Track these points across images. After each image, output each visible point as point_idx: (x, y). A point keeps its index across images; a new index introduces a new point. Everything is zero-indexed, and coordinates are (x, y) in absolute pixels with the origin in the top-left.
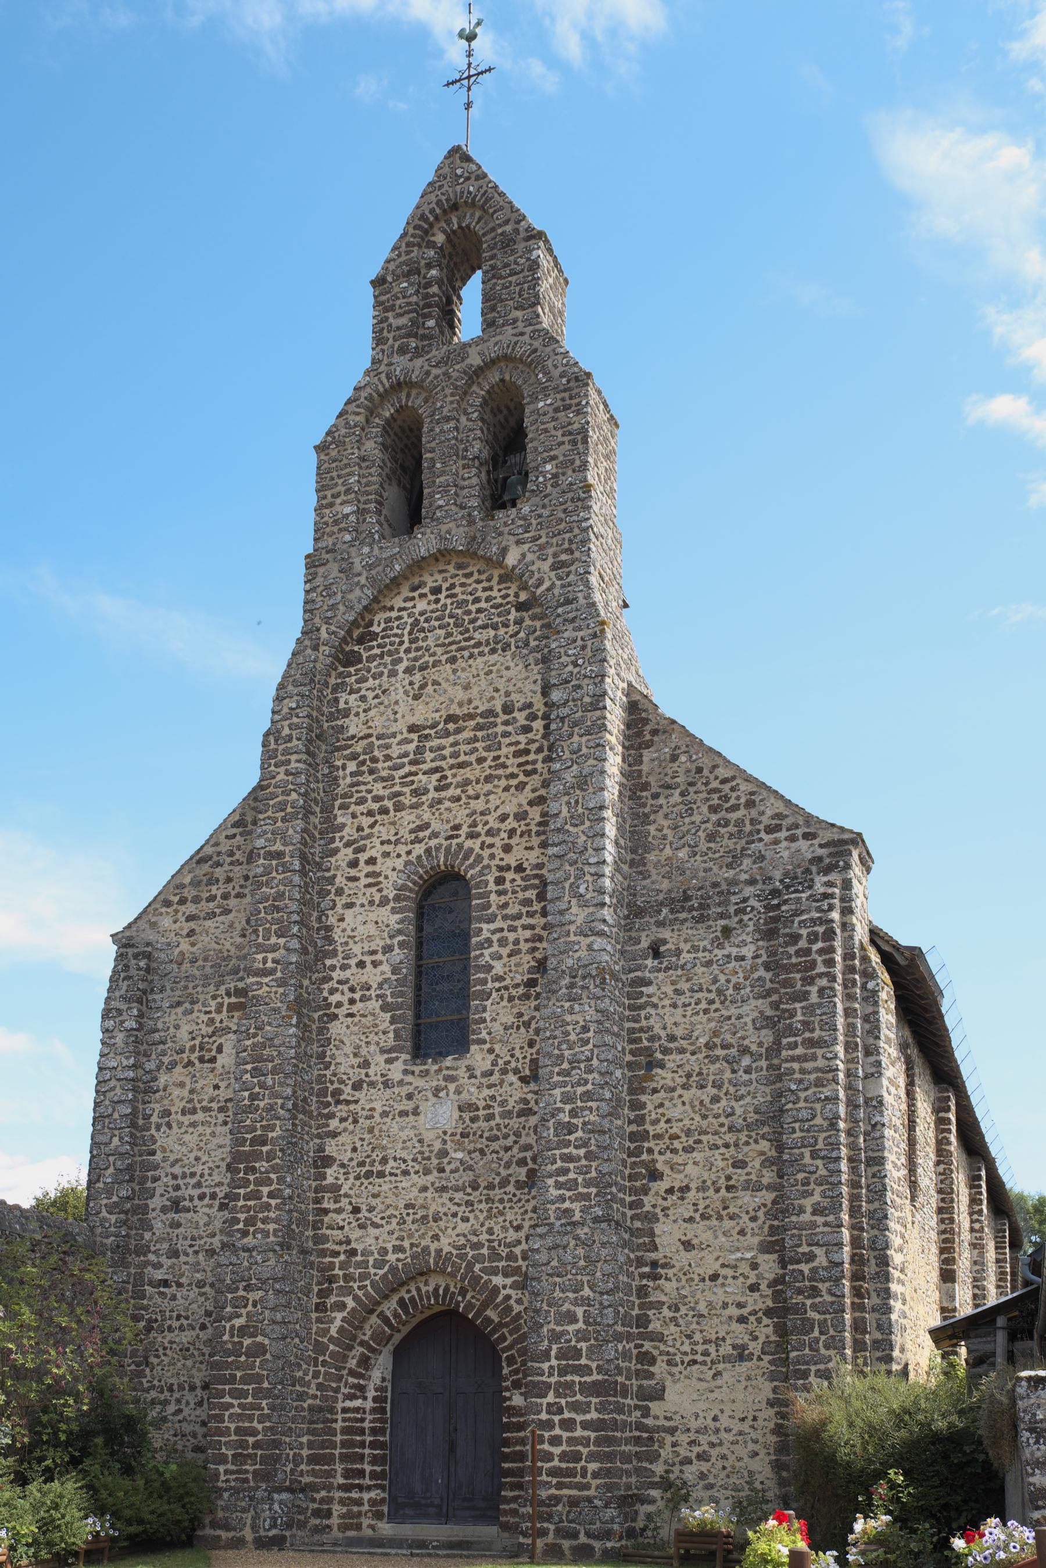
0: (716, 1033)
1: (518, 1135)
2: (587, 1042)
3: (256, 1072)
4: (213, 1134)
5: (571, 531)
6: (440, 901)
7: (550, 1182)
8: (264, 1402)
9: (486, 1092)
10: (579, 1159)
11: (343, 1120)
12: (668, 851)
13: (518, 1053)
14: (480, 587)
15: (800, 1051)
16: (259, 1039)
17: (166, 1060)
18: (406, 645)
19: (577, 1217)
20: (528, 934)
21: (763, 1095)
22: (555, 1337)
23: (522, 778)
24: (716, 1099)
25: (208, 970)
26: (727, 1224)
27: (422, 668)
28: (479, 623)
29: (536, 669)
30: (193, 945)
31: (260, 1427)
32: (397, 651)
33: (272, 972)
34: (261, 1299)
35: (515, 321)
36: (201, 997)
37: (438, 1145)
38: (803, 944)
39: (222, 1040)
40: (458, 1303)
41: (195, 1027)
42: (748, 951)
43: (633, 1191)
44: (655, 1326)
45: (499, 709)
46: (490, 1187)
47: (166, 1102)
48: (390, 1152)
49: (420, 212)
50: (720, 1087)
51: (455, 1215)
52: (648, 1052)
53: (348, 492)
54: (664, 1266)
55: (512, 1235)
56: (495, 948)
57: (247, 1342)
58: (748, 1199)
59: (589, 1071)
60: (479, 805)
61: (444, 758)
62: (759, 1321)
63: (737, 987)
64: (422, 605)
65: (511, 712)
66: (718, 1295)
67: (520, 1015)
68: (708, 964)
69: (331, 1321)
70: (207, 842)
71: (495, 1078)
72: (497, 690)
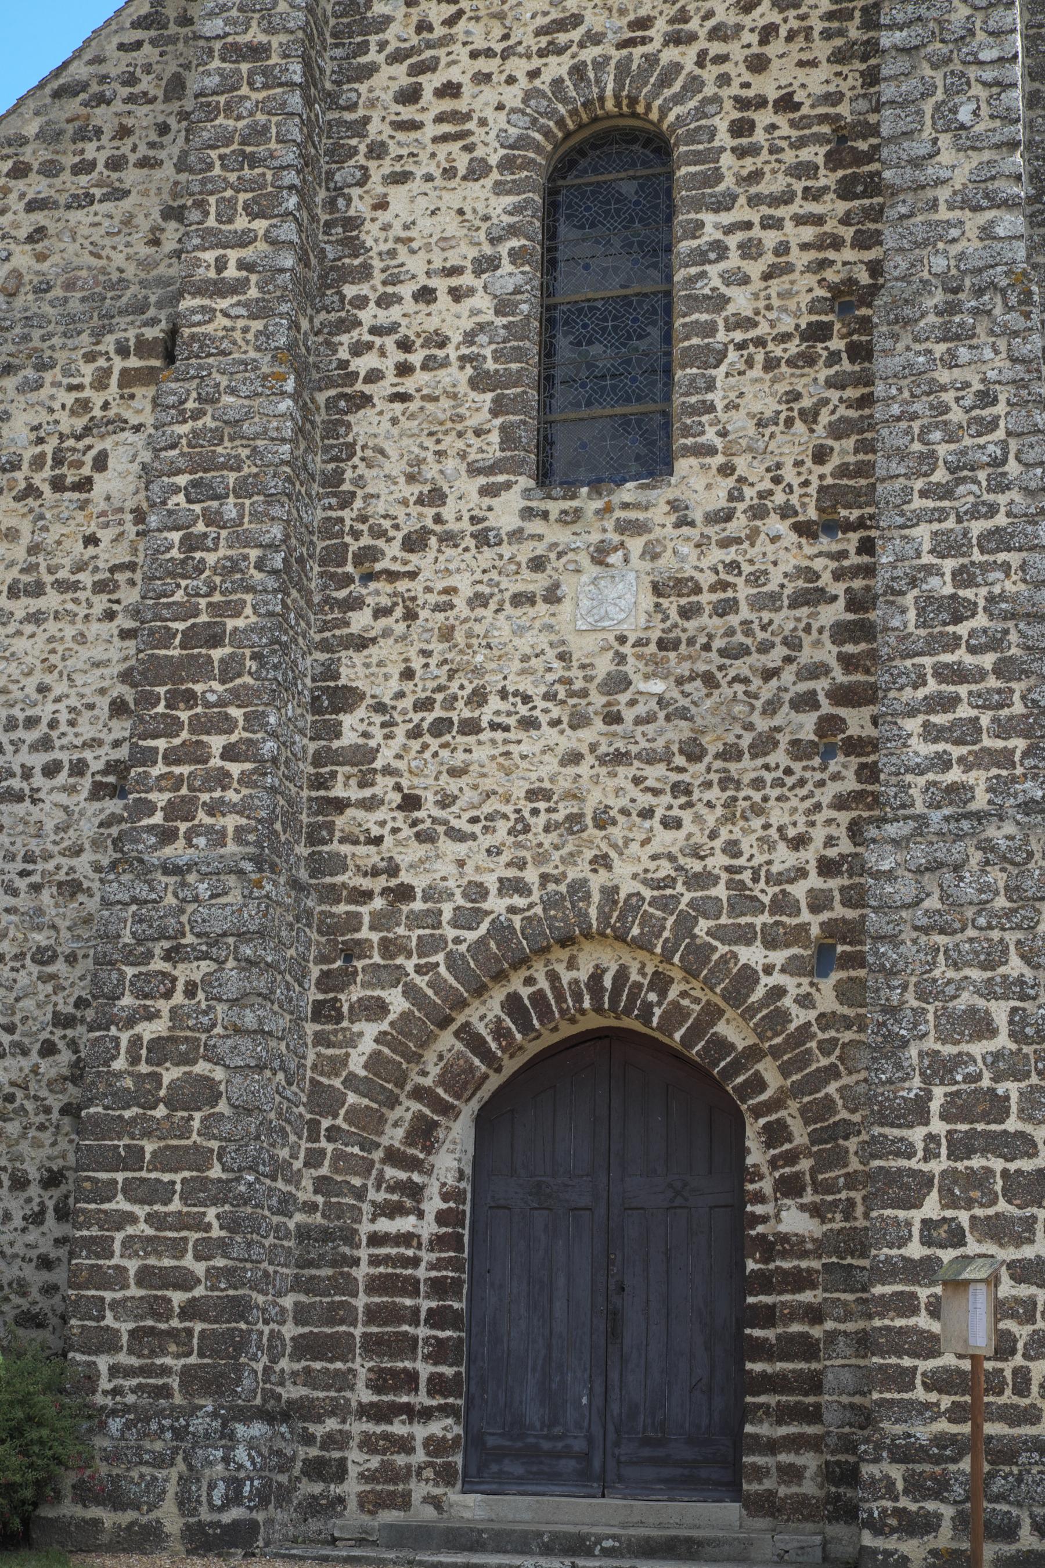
1: (793, 643)
3: (197, 491)
4: (81, 638)
8: (211, 1214)
9: (716, 555)
11: (380, 612)
13: (789, 474)
16: (208, 421)
20: (808, 233)
25: (75, 306)
30: (41, 257)
31: (199, 1269)
34: (207, 980)
36: (61, 357)
37: (604, 666)
39: (107, 444)
40: (647, 1009)
41: (44, 417)
46: (730, 753)
48: (493, 681)
51: (647, 813)
55: (784, 858)
56: (734, 260)
57: (171, 1074)
67: (794, 396)
69: (352, 1041)
70: (78, 54)
71: (738, 525)
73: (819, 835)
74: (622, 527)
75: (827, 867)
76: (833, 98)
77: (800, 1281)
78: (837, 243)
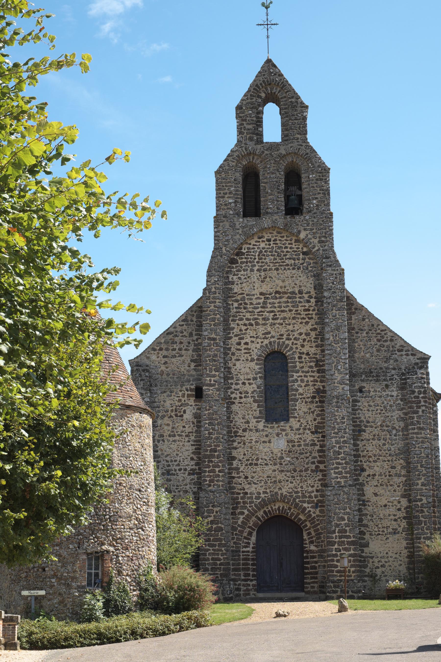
0: (384, 421)
1: (311, 452)
2: (344, 423)
4: (183, 445)
5: (325, 229)
6: (275, 362)
7: (332, 471)
9: (298, 436)
10: (342, 464)
12: (362, 354)
14: (287, 242)
15: (416, 431)
17: (160, 414)
18: (257, 260)
19: (343, 484)
20: (312, 379)
21: (401, 444)
22: (337, 525)
23: (307, 320)
24: (384, 445)
26: (390, 488)
27: (265, 270)
28: (288, 257)
29: (311, 279)
30: (167, 368)
31: (222, 558)
32: (253, 262)
33: (214, 385)
34: (219, 511)
35: (298, 139)
36: (175, 390)
37: (279, 455)
38: (416, 394)
39: (185, 408)
40: (288, 513)
41: (173, 402)
42: (395, 394)
43: (356, 475)
44: (365, 522)
45: (297, 292)
46: (301, 471)
47: (161, 431)
48: (260, 457)
49: (256, 83)
50: (386, 440)
51: (287, 481)
52: (359, 426)
53: (230, 193)
54: (368, 501)
55: (310, 489)
56: (299, 383)
57: (214, 526)
58: (396, 480)
59: (345, 433)
60: (290, 327)
61: (275, 307)
62: (401, 520)
63: (391, 406)
64: (262, 245)
65: (302, 294)
66: (387, 512)
68: (380, 397)
69: (239, 519)
70: (171, 326)
71: (301, 431)
72: (296, 284)
73: (316, 485)
75: (317, 491)
76: (316, 354)
77: (314, 557)
78: (317, 381)
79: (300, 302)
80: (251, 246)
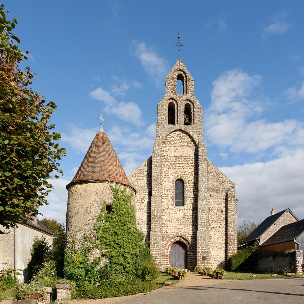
4: (144, 214)
7: (200, 225)
8: (159, 253)
9: (187, 212)
11: (165, 214)
22: (201, 245)
23: (192, 167)
24: (218, 216)
25: (141, 188)
26: (219, 232)
27: (176, 147)
33: (156, 191)
35: (190, 94)
36: (141, 192)
38: (231, 198)
44: (210, 244)
46: (188, 225)
48: (173, 219)
53: (163, 114)
57: (156, 244)
64: (175, 137)
66: (218, 241)
69: (164, 242)
71: (188, 210)
74: (181, 209)
77: (191, 257)
79: (189, 160)
80: (171, 137)
